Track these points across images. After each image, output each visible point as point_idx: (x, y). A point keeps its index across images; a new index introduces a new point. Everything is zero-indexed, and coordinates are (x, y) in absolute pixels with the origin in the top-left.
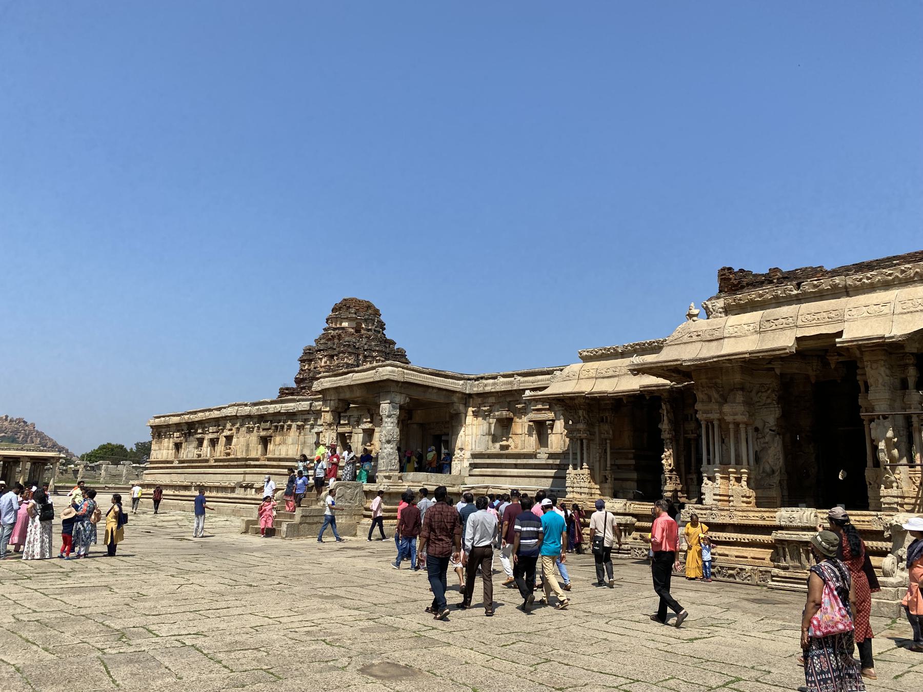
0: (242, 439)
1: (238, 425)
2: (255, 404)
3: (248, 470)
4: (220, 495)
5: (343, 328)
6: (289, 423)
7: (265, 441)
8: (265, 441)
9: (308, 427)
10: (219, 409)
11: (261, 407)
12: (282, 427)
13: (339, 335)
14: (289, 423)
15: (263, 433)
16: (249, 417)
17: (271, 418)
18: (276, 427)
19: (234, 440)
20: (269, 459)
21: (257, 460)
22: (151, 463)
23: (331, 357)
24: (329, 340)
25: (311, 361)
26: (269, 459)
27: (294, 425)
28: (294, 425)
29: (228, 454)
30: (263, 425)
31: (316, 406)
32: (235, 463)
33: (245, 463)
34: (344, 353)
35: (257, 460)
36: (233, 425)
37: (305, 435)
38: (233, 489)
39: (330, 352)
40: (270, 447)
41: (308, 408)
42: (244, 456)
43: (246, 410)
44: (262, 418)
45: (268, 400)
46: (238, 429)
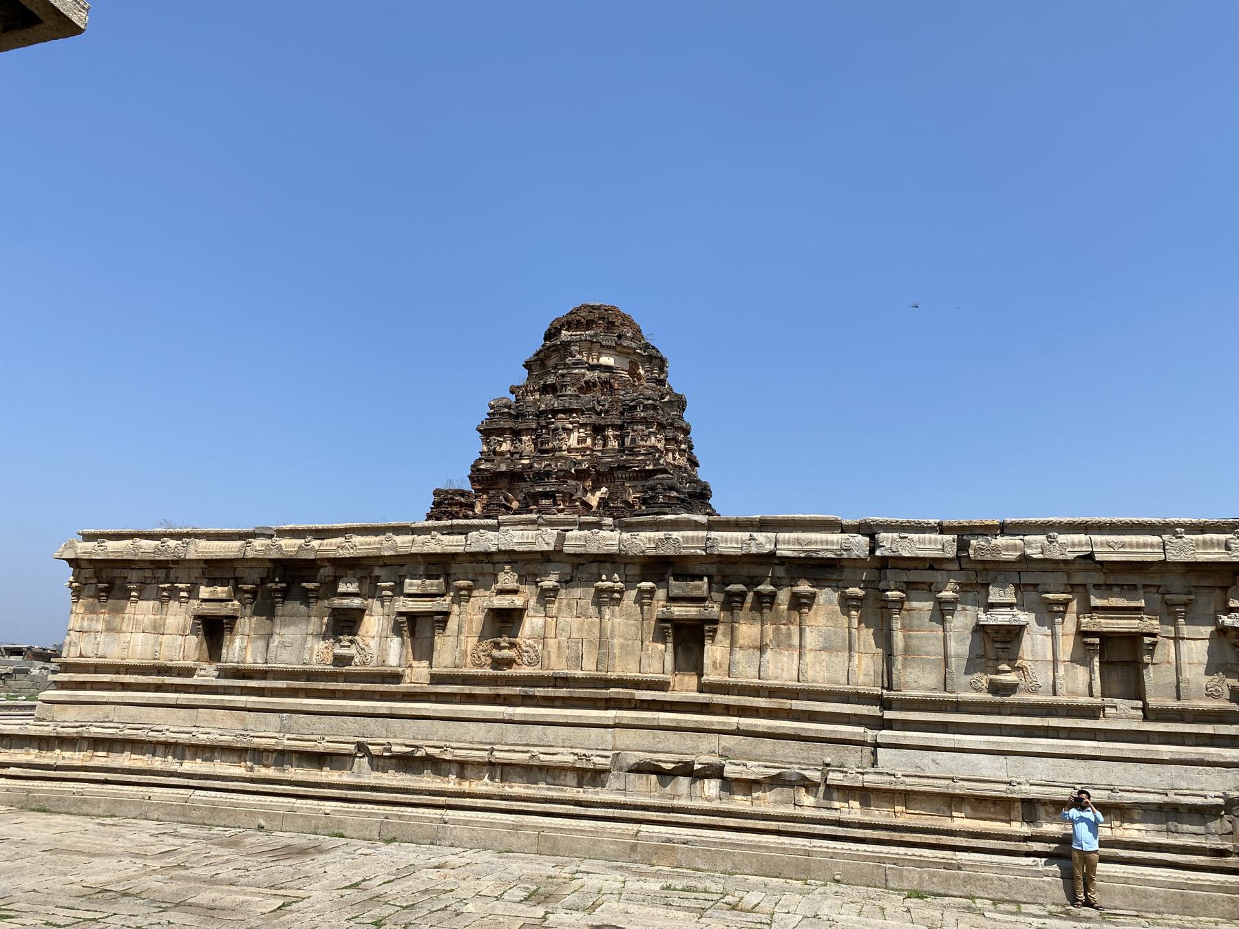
1: (549, 582)
4: (518, 789)
5: (608, 368)
11: (675, 535)
13: (605, 383)
14: (804, 587)
17: (713, 569)
19: (531, 624)
23: (598, 430)
25: (516, 434)
28: (827, 597)
30: (677, 587)
31: (996, 549)
32: (551, 692)
34: (646, 422)
38: (595, 776)
39: (594, 419)
40: (714, 652)
41: (951, 552)
42: (588, 668)
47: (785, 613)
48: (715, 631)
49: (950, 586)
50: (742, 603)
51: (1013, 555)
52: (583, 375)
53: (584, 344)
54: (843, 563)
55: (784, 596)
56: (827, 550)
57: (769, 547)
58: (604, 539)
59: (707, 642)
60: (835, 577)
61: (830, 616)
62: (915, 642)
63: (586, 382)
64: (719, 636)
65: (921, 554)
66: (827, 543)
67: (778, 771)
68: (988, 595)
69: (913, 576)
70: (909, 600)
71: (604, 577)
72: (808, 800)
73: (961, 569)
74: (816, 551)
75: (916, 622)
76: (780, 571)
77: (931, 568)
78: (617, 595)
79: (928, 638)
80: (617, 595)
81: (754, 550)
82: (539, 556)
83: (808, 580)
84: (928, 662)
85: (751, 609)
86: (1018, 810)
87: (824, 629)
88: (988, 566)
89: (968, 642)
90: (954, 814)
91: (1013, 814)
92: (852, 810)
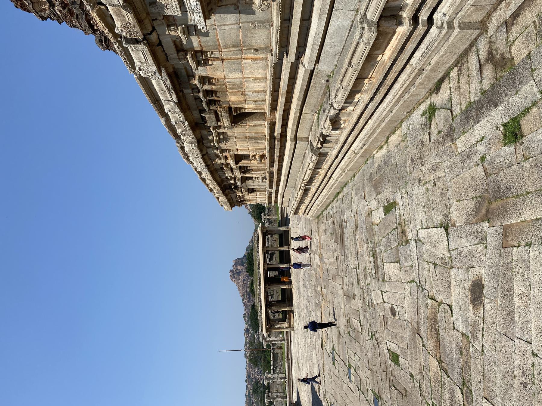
0: (238, 146)
1: (218, 152)
2: (177, 137)
3: (289, 135)
6: (196, 82)
7: (238, 117)
8: (238, 117)
9: (195, 42)
10: (200, 173)
12: (208, 93)
14: (196, 82)
15: (226, 122)
16: (201, 143)
17: (196, 114)
18: (210, 103)
20: (274, 108)
21: (273, 125)
22: (270, 202)
24: (71, 12)
26: (274, 108)
27: (201, 71)
29: (263, 157)
31: (127, 26)
33: (277, 141)
35: (273, 125)
36: (218, 156)
37: (218, 47)
40: (249, 107)
41: (142, 47)
43: (190, 147)
44: (198, 126)
45: (163, 121)
46: (223, 151)
47: (219, 86)
48: (236, 109)
49: (173, 33)
50: (215, 101)
51: (129, 17)
52: (60, 11)
53: (37, 10)
54: (171, 70)
55: (206, 87)
56: (165, 84)
57: (172, 104)
58: (190, 150)
59: (243, 111)
60: (184, 72)
61: (214, 69)
62: (229, 43)
63: (64, 8)
64: (240, 106)
65: (150, 61)
66: (159, 84)
67: (328, 122)
68: (173, 17)
69: (171, 51)
70: (194, 48)
71: (212, 144)
72: (350, 108)
73: (154, 29)
74: (168, 88)
75: (211, 43)
76: (188, 92)
77: (160, 44)
78: (221, 137)
79: (224, 39)
80: (221, 137)
81: (177, 110)
82: (206, 156)
83: (189, 81)
84: (245, 36)
85: (218, 97)
86: (386, 25)
87: (226, 72)
88: (144, 15)
89: (223, 16)
90: (378, 59)
91: (388, 31)
92: (362, 98)
